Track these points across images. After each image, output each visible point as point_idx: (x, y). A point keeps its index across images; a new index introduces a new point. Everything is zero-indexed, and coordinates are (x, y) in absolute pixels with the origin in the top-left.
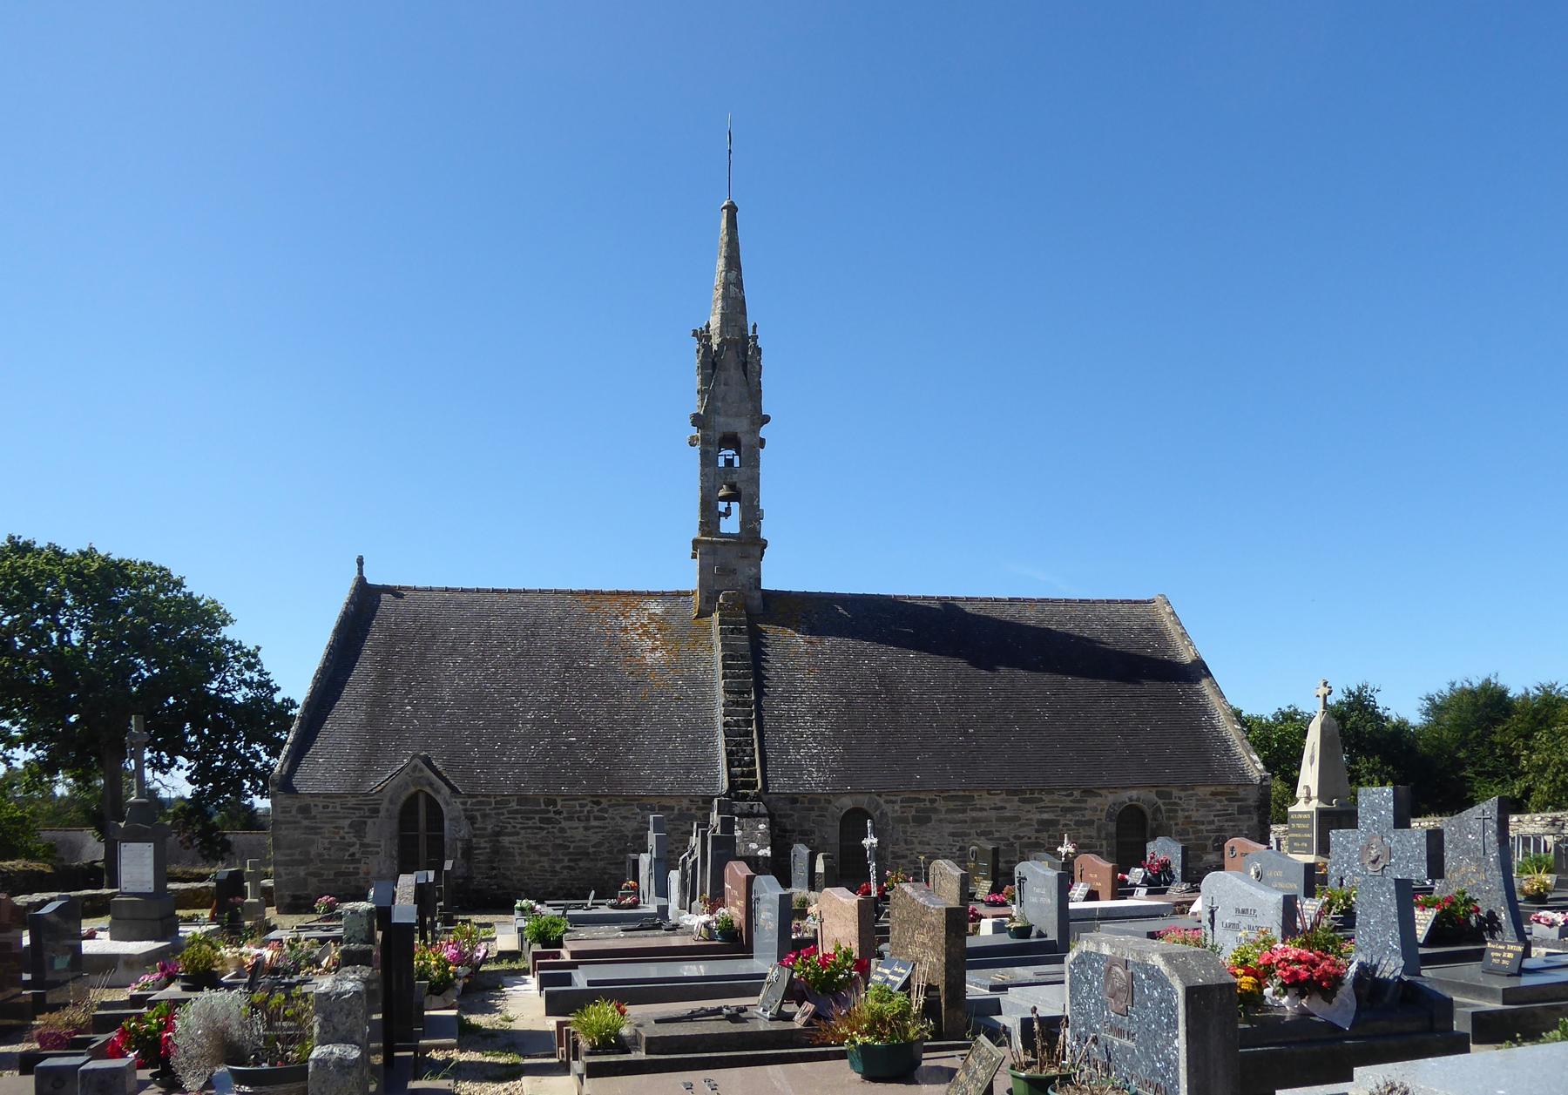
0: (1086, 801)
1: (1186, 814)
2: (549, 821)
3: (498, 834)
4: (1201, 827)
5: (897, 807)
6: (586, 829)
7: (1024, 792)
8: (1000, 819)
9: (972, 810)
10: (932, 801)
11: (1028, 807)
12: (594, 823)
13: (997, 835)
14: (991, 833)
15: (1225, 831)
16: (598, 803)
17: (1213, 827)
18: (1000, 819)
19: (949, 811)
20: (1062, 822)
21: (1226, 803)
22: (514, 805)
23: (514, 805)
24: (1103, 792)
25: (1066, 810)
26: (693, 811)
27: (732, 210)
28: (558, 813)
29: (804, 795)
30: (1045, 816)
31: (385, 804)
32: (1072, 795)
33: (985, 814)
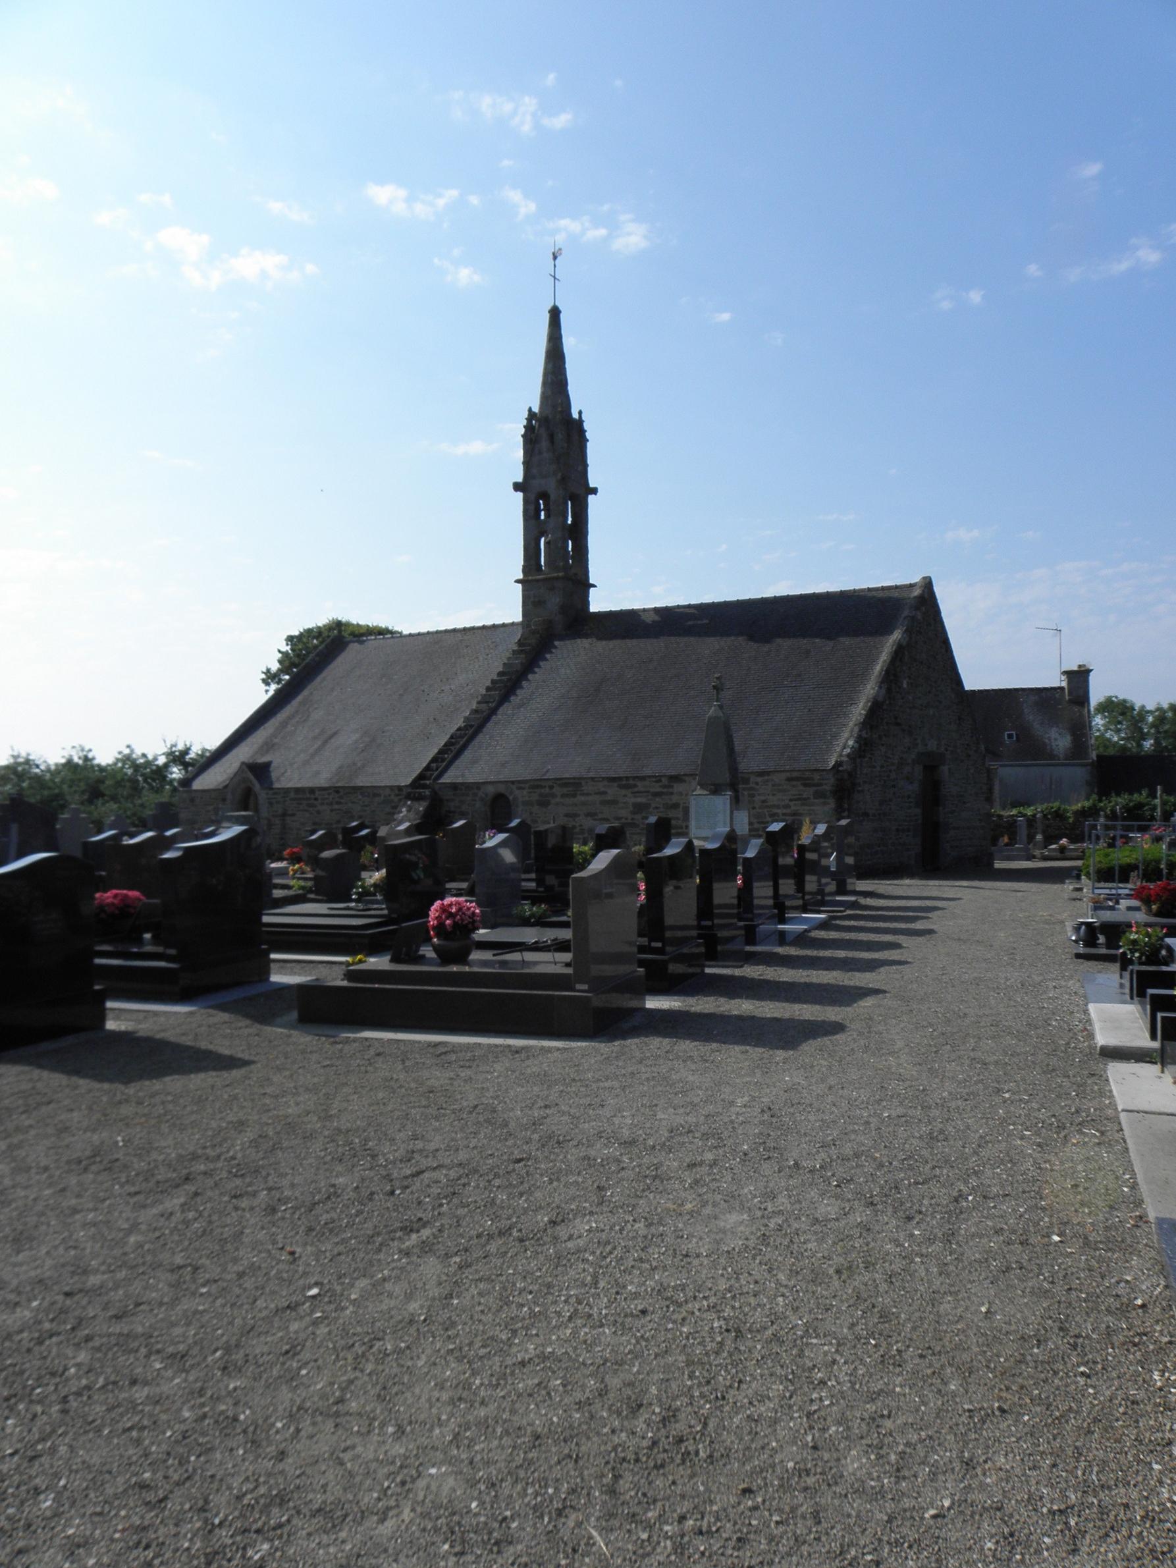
0: (672, 787)
1: (763, 798)
2: (310, 805)
3: (284, 815)
4: (779, 811)
5: (525, 792)
6: (332, 810)
7: (620, 779)
8: (604, 803)
9: (583, 794)
10: (551, 787)
11: (624, 792)
12: (336, 807)
13: (600, 816)
14: (595, 814)
15: (801, 815)
16: (338, 792)
17: (788, 811)
18: (604, 803)
19: (563, 796)
20: (653, 805)
21: (801, 788)
22: (292, 795)
23: (292, 795)
24: (687, 778)
25: (656, 794)
26: (392, 797)
27: (555, 313)
28: (316, 799)
29: (462, 784)
30: (639, 800)
31: (229, 796)
32: (660, 781)
33: (590, 798)
